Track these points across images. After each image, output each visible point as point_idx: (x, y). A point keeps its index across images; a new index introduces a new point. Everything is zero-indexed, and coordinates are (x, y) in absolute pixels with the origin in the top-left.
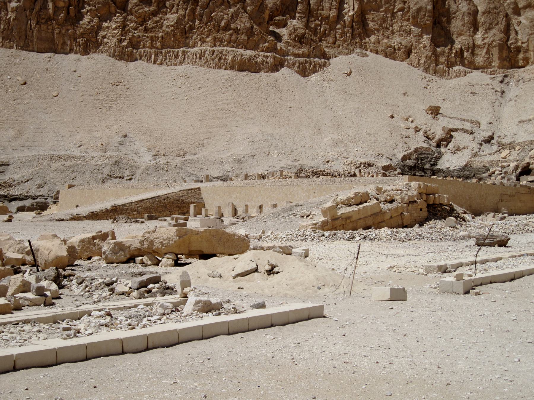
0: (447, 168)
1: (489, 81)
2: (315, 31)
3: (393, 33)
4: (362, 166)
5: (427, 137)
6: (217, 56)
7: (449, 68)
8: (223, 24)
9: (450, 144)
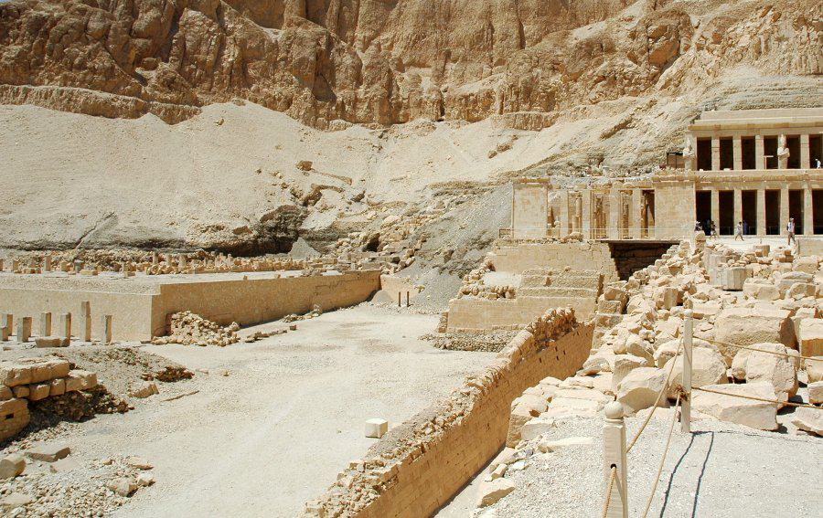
1: (369, 136)
2: (188, 77)
3: (274, 82)
6: (66, 97)
7: (329, 121)
8: (77, 61)
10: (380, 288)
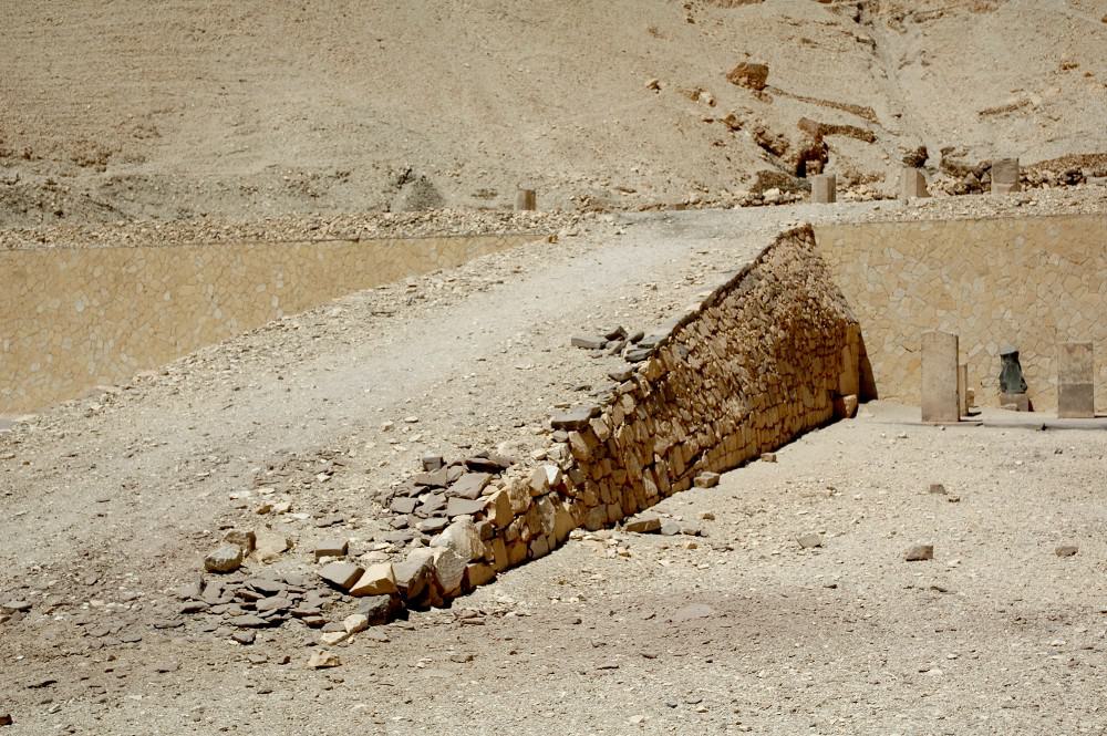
1: (831, 17)
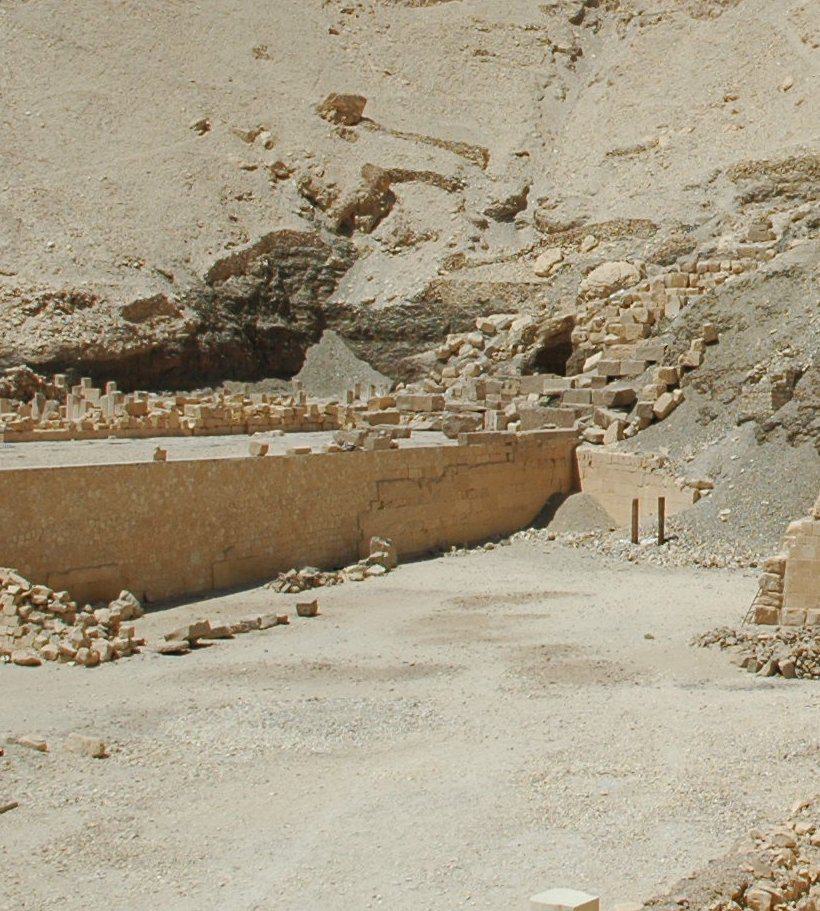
0: (367, 303)
4: (51, 304)
5: (310, 198)
9: (385, 220)
10: (575, 486)
